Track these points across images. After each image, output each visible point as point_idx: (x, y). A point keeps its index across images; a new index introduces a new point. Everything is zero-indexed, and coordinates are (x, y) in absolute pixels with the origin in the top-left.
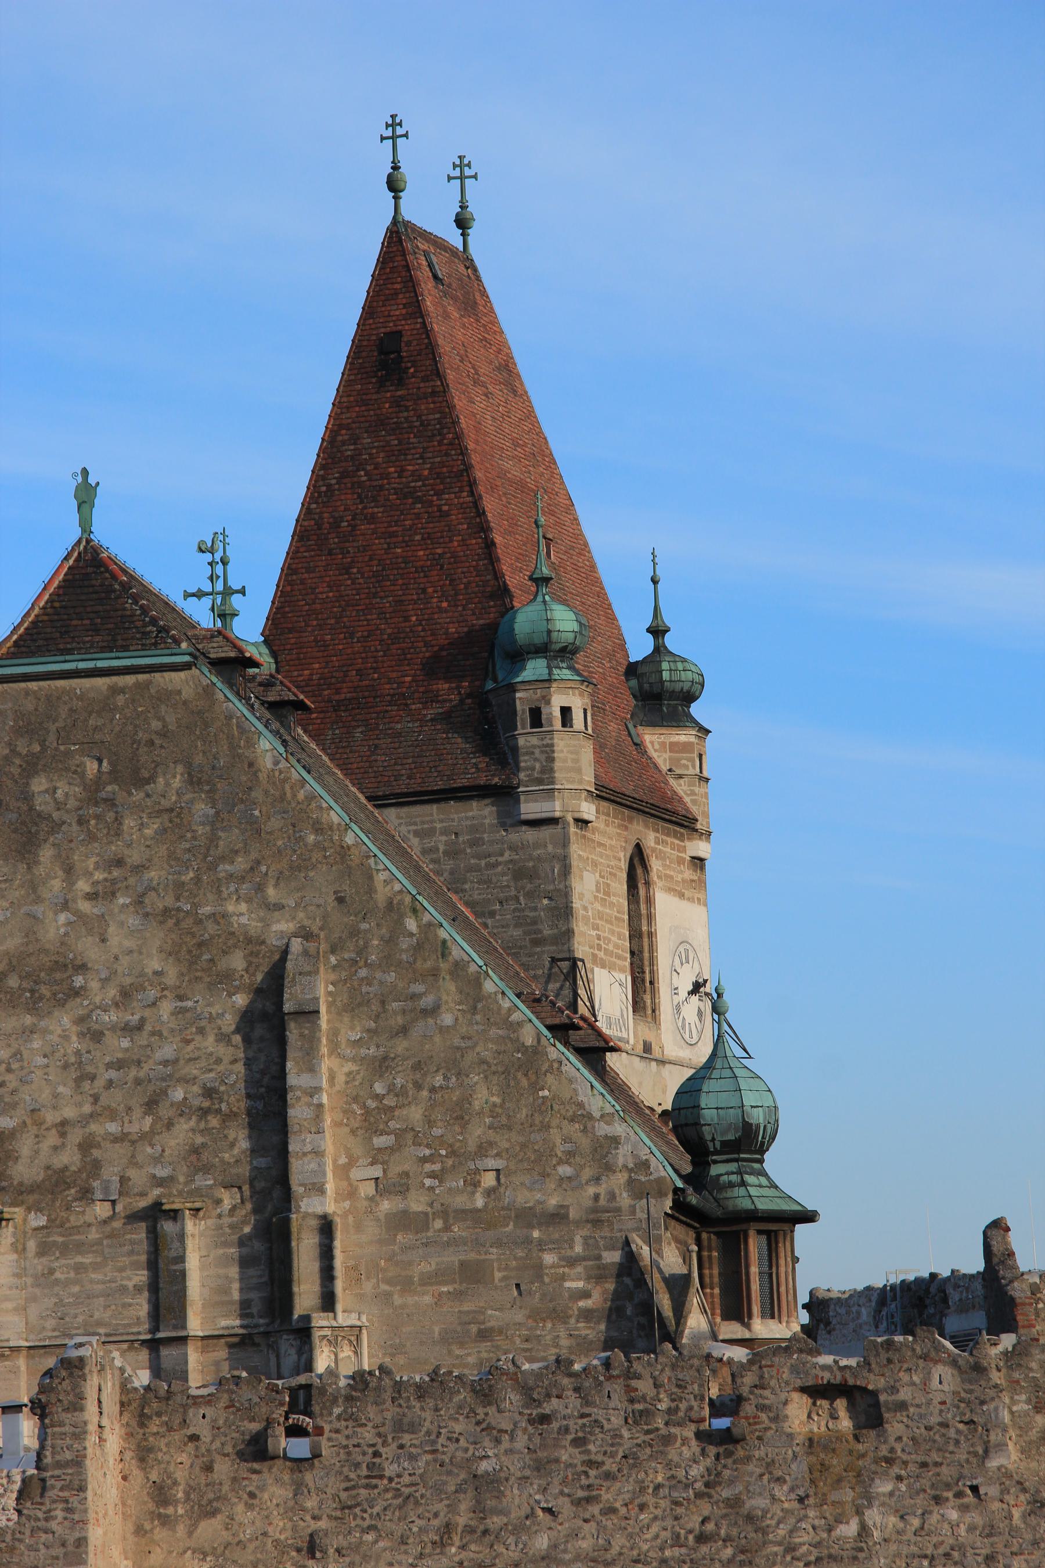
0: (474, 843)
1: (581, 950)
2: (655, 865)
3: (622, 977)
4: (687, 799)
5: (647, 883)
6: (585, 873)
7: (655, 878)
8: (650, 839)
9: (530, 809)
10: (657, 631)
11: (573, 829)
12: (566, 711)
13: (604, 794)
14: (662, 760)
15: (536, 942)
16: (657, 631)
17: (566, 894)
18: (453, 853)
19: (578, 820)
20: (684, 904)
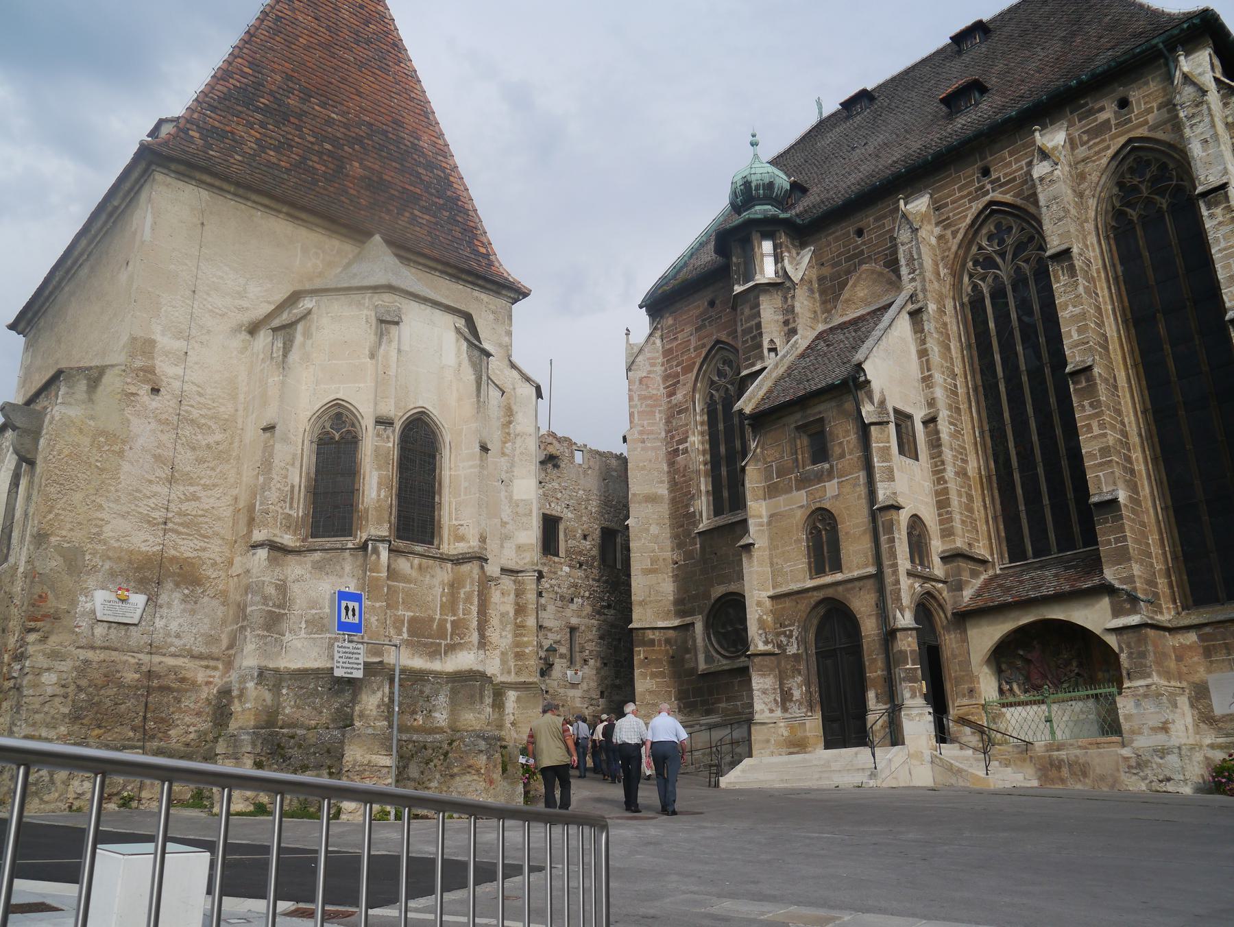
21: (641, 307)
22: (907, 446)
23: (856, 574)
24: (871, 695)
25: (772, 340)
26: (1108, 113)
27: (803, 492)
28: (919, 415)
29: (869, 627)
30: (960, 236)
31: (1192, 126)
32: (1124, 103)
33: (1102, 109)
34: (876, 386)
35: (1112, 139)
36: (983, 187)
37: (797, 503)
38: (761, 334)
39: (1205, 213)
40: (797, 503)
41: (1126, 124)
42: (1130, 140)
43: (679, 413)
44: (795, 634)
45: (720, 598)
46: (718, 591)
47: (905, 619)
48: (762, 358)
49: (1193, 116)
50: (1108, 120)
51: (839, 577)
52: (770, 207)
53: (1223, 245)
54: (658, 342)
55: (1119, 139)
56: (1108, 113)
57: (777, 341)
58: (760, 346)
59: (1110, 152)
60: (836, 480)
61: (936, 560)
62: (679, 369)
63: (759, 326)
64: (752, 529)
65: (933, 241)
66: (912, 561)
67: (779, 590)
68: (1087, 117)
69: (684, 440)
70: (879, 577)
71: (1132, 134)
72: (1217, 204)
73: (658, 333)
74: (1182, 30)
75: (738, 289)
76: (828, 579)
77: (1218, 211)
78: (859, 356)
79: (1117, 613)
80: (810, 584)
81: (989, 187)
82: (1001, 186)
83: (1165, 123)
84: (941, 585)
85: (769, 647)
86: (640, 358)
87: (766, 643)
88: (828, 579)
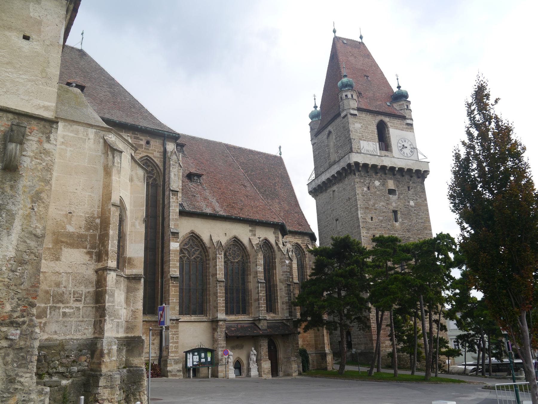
0: (338, 126)
1: (352, 136)
2: (389, 124)
3: (375, 143)
4: (403, 113)
5: (387, 128)
6: (355, 124)
7: (390, 126)
8: (386, 119)
9: (343, 115)
10: (399, 87)
11: (349, 116)
12: (346, 96)
13: (359, 109)
14: (398, 108)
15: (346, 139)
16: (399, 87)
17: (349, 128)
18: (336, 129)
19: (352, 114)
26: (143, 143)
31: (173, 168)
32: (148, 143)
33: (142, 140)
35: (142, 152)
39: (171, 196)
41: (147, 150)
42: (147, 156)
49: (174, 165)
50: (142, 145)
53: (173, 208)
55: (144, 153)
68: (136, 139)
71: (148, 155)
72: (175, 195)
74: (173, 135)
77: (175, 197)
83: (158, 158)
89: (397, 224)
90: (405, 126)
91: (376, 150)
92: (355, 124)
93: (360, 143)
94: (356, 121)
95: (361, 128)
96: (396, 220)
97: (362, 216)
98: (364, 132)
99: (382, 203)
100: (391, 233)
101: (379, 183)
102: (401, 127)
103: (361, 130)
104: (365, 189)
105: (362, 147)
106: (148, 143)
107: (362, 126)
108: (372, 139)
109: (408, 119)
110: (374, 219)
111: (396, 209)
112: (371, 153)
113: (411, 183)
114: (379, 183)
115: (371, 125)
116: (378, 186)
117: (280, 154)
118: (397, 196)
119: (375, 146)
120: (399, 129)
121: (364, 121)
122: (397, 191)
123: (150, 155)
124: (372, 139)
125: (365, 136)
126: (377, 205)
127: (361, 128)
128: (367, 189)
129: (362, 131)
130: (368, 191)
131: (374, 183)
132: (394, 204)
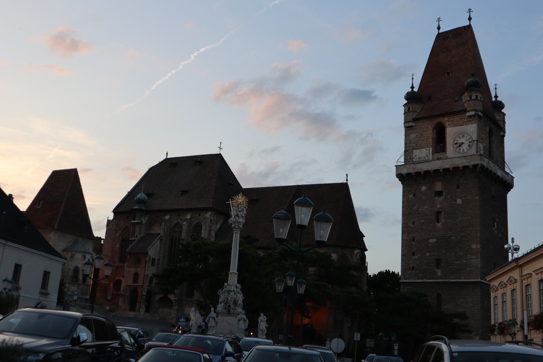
3: (428, 149)
20: (462, 127)
21: (112, 212)
22: (153, 264)
23: (140, 284)
24: (138, 304)
25: (137, 234)
26: (197, 215)
27: (135, 269)
28: (157, 258)
29: (140, 294)
30: (173, 226)
32: (200, 215)
33: (197, 214)
34: (149, 254)
36: (178, 218)
37: (133, 270)
38: (135, 233)
40: (133, 270)
43: (116, 239)
44: (128, 292)
45: (117, 280)
46: (117, 278)
47: (144, 293)
48: (134, 237)
51: (137, 284)
52: (142, 205)
54: (115, 221)
56: (197, 215)
57: (138, 234)
58: (134, 235)
59: (196, 222)
60: (140, 268)
61: (154, 283)
62: (118, 229)
63: (135, 231)
64: (125, 273)
65: (168, 225)
66: (149, 284)
67: (127, 284)
69: (116, 245)
70: (143, 285)
73: (115, 219)
75: (133, 222)
76: (135, 284)
78: (147, 250)
79: (175, 297)
80: (132, 284)
81: (179, 219)
82: (181, 220)
84: (153, 288)
85: (124, 294)
86: (110, 224)
87: (123, 293)
88: (135, 284)
89: (439, 225)
90: (466, 120)
91: (428, 155)
92: (411, 135)
93: (413, 153)
94: (412, 132)
95: (415, 138)
96: (438, 222)
97: (405, 221)
98: (419, 140)
99: (427, 207)
100: (431, 234)
101: (426, 188)
102: (461, 122)
103: (416, 139)
104: (411, 196)
105: (414, 156)
106: (200, 215)
107: (417, 136)
108: (427, 145)
109: (469, 111)
110: (415, 223)
111: (440, 210)
112: (423, 159)
113: (461, 180)
114: (426, 188)
115: (426, 131)
116: (424, 191)
117: (347, 180)
118: (443, 197)
119: (428, 152)
120: (458, 126)
121: (420, 129)
122: (444, 192)
123: (200, 221)
124: (427, 145)
125: (419, 144)
126: (420, 210)
127: (415, 138)
128: (413, 196)
129: (417, 141)
130: (414, 198)
131: (421, 188)
132: (438, 206)
